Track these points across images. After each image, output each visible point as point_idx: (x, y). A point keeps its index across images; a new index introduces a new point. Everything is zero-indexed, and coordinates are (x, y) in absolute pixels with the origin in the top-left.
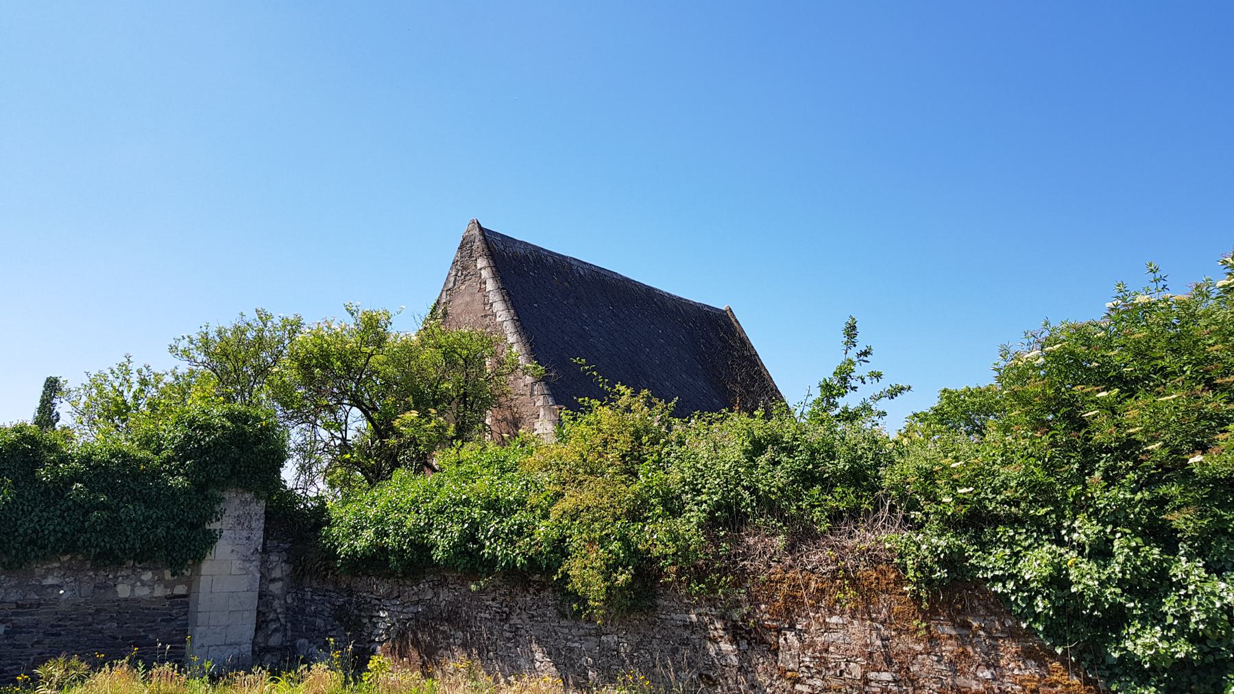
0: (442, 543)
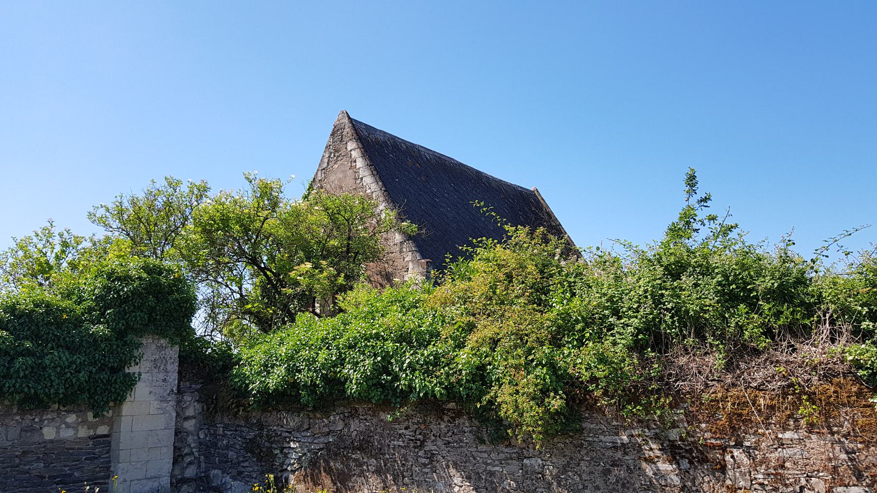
0: (355, 376)
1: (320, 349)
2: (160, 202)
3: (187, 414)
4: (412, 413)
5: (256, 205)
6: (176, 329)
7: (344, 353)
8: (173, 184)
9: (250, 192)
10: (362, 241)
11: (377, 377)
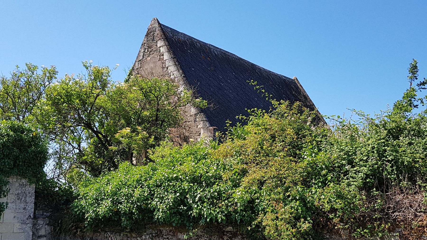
0: (162, 207)
1: (136, 188)
2: (22, 82)
3: (40, 234)
4: (201, 234)
5: (91, 85)
6: (33, 172)
7: (154, 190)
8: (32, 69)
9: (87, 75)
10: (167, 113)
11: (176, 208)
